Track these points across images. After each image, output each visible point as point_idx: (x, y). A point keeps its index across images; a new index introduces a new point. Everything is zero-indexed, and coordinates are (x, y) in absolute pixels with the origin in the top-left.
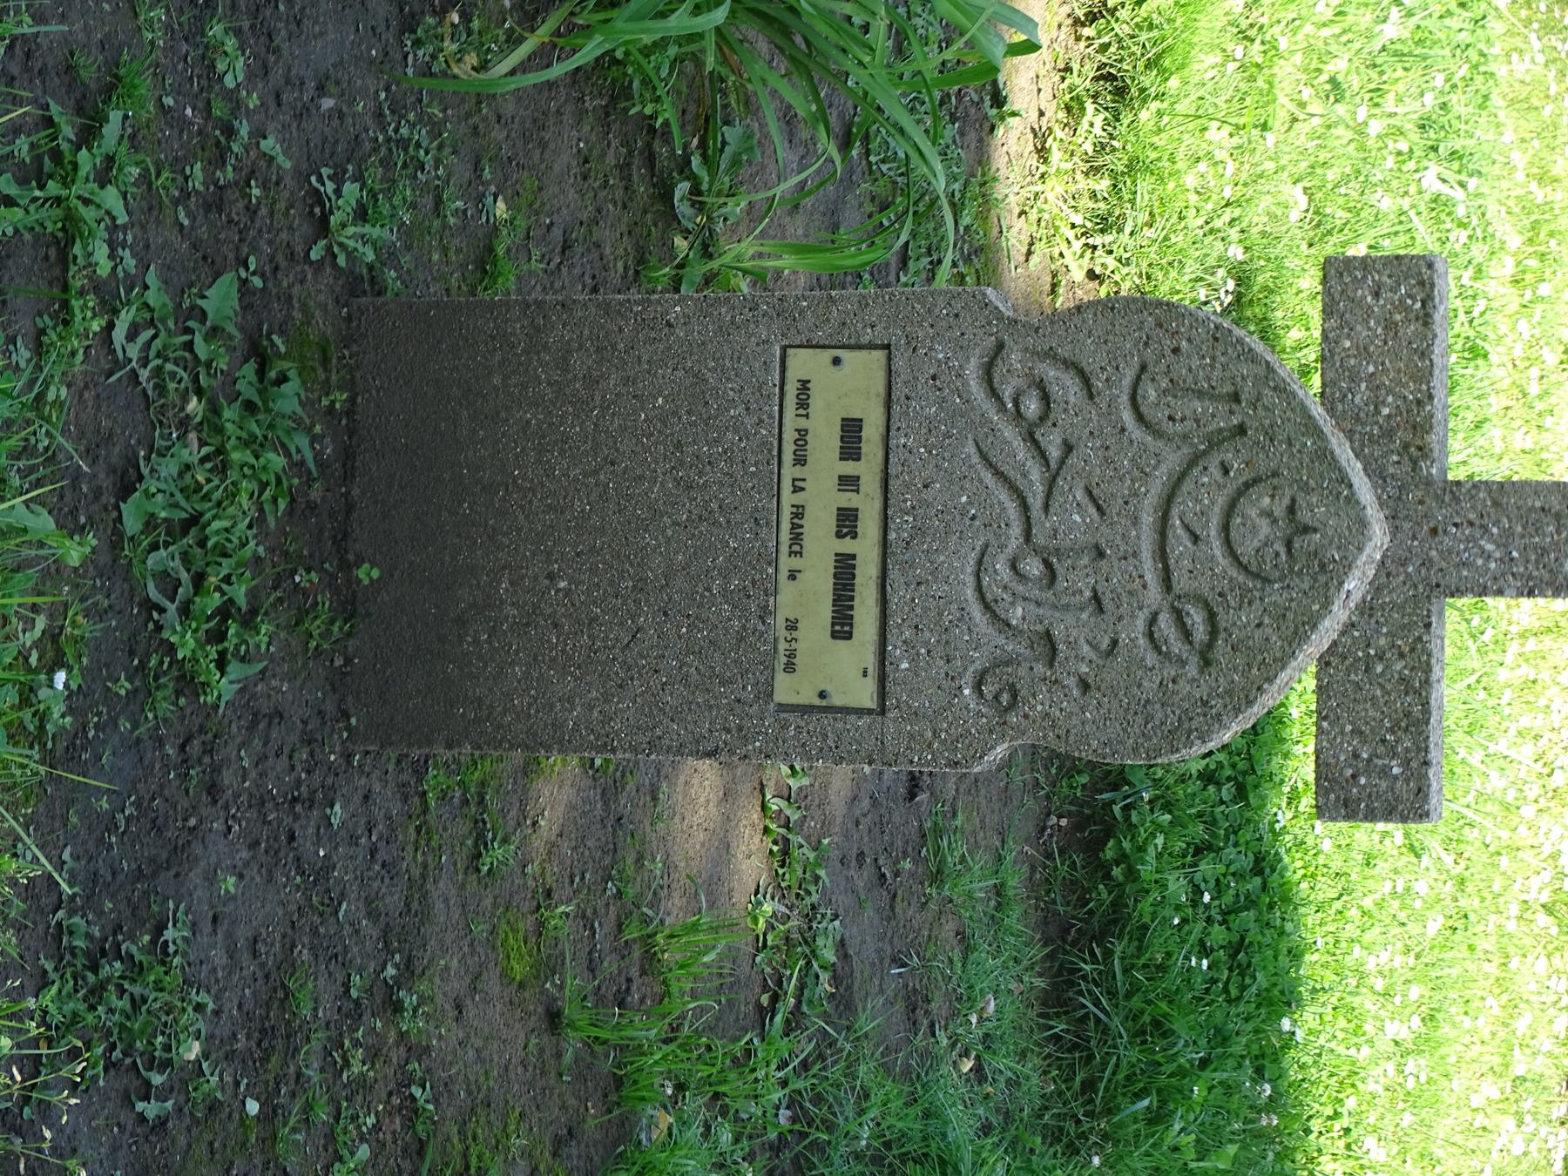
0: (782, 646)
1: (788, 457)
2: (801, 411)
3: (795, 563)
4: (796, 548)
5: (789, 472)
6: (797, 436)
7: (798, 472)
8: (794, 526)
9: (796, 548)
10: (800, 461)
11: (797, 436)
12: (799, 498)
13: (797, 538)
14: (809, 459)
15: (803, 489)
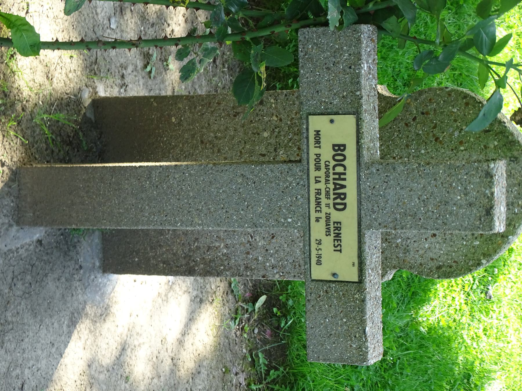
0: (314, 253)
1: (312, 167)
2: (317, 145)
3: (318, 215)
4: (318, 209)
5: (313, 174)
6: (315, 157)
7: (318, 173)
8: (317, 199)
9: (318, 209)
10: (318, 168)
11: (315, 157)
12: (318, 186)
13: (318, 204)
14: (321, 167)
15: (320, 182)
